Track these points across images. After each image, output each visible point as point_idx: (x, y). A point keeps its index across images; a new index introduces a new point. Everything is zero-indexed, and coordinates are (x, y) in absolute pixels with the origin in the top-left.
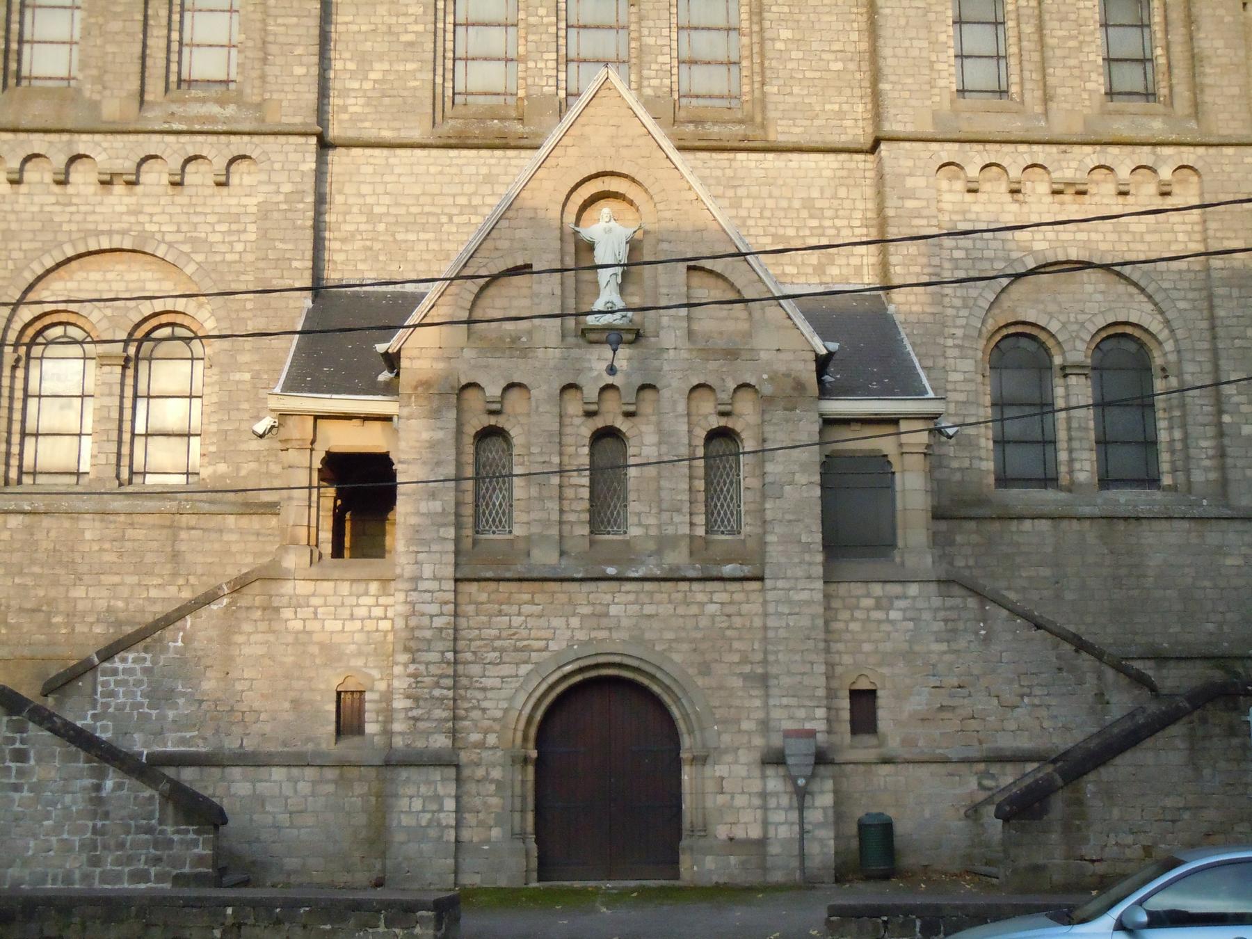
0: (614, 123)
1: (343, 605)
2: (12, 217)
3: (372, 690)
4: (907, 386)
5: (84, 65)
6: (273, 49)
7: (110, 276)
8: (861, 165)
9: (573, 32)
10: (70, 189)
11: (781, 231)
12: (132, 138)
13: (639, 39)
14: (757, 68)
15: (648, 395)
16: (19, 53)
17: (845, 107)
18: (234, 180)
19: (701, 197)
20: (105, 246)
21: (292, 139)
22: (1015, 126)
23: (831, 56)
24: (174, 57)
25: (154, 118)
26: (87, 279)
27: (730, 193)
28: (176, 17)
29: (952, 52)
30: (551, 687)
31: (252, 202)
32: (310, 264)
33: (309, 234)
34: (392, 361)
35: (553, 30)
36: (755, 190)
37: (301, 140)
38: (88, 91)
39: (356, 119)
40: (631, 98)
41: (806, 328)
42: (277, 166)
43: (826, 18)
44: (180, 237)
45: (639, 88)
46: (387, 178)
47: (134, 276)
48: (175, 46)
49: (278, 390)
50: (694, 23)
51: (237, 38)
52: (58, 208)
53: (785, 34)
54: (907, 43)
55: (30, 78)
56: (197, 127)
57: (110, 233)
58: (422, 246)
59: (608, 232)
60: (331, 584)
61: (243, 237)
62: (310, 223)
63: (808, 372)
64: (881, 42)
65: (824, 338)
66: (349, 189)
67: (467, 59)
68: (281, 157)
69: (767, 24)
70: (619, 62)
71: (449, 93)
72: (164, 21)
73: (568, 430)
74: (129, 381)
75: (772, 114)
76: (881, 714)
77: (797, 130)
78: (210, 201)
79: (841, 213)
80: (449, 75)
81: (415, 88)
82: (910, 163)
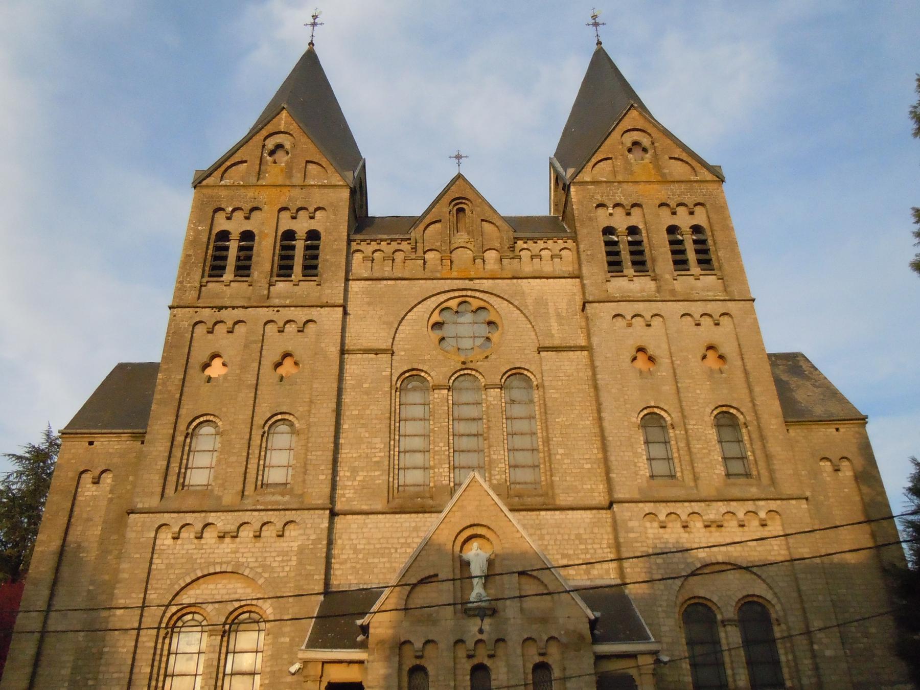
0: (478, 498)
2: (172, 557)
4: (638, 634)
5: (216, 478)
6: (310, 467)
7: (219, 586)
8: (604, 516)
9: (457, 454)
10: (203, 541)
11: (566, 552)
12: (236, 514)
13: (489, 456)
14: (548, 468)
15: (501, 644)
16: (185, 473)
17: (594, 486)
18: (287, 533)
19: (522, 534)
20: (218, 570)
21: (317, 512)
22: (680, 493)
23: (585, 461)
24: (261, 473)
25: (248, 503)
26: (207, 589)
27: (538, 532)
28: (263, 453)
29: (645, 457)
31: (295, 545)
32: (323, 577)
33: (323, 561)
34: (365, 629)
35: (447, 453)
36: (551, 530)
37: (321, 512)
38: (217, 491)
39: (349, 500)
40: (486, 486)
41: (582, 604)
42: (309, 526)
43: (581, 443)
44: (257, 564)
45: (490, 480)
46: (364, 530)
47: (231, 586)
48: (261, 468)
49: (303, 647)
50: (516, 447)
51: (292, 462)
52: (195, 551)
53: (561, 451)
54: (622, 454)
55: (189, 486)
56: (270, 507)
57: (221, 563)
58: (381, 565)
59: (476, 554)
61: (289, 563)
62: (324, 555)
63: (585, 629)
64: (609, 454)
65: (592, 611)
66: (344, 537)
67: (405, 469)
68: (311, 521)
69: (551, 447)
70: (480, 468)
71: (396, 486)
72: (257, 456)
73: (458, 666)
74: (225, 644)
75: (557, 491)
77: (571, 499)
78: (273, 545)
79: (596, 541)
80: (396, 477)
81: (379, 484)
82: (629, 514)
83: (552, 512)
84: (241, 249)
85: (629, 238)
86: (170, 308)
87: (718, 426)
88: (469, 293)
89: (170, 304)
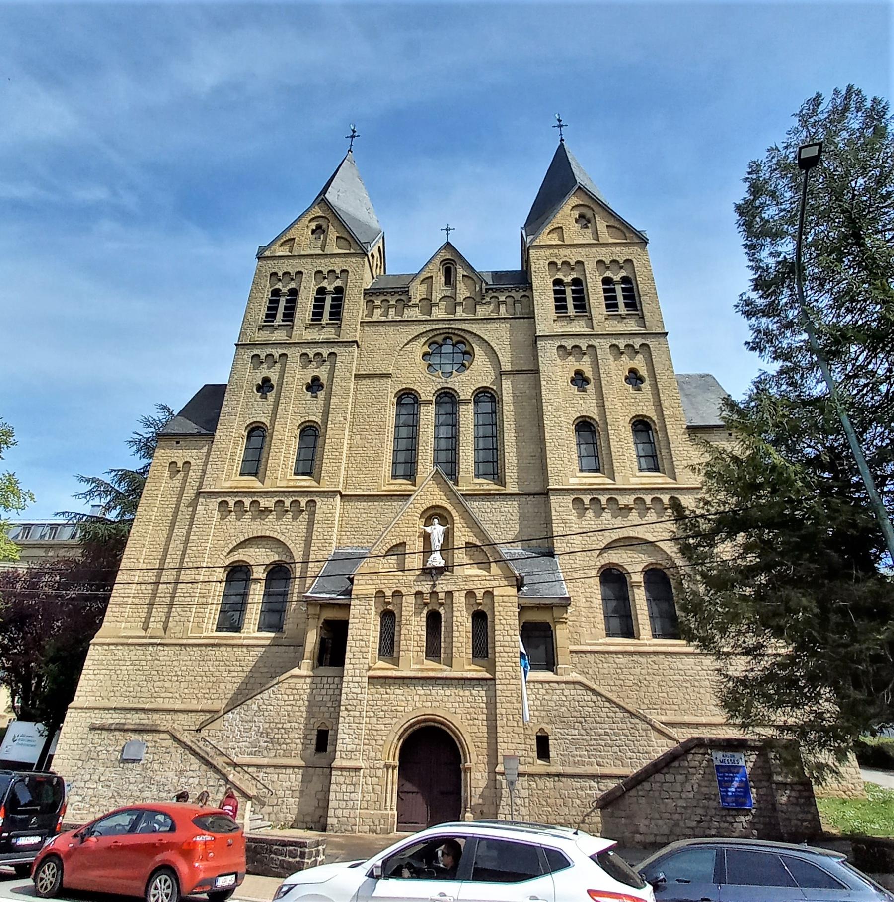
30: (405, 730)
84: (287, 301)
88: (450, 331)
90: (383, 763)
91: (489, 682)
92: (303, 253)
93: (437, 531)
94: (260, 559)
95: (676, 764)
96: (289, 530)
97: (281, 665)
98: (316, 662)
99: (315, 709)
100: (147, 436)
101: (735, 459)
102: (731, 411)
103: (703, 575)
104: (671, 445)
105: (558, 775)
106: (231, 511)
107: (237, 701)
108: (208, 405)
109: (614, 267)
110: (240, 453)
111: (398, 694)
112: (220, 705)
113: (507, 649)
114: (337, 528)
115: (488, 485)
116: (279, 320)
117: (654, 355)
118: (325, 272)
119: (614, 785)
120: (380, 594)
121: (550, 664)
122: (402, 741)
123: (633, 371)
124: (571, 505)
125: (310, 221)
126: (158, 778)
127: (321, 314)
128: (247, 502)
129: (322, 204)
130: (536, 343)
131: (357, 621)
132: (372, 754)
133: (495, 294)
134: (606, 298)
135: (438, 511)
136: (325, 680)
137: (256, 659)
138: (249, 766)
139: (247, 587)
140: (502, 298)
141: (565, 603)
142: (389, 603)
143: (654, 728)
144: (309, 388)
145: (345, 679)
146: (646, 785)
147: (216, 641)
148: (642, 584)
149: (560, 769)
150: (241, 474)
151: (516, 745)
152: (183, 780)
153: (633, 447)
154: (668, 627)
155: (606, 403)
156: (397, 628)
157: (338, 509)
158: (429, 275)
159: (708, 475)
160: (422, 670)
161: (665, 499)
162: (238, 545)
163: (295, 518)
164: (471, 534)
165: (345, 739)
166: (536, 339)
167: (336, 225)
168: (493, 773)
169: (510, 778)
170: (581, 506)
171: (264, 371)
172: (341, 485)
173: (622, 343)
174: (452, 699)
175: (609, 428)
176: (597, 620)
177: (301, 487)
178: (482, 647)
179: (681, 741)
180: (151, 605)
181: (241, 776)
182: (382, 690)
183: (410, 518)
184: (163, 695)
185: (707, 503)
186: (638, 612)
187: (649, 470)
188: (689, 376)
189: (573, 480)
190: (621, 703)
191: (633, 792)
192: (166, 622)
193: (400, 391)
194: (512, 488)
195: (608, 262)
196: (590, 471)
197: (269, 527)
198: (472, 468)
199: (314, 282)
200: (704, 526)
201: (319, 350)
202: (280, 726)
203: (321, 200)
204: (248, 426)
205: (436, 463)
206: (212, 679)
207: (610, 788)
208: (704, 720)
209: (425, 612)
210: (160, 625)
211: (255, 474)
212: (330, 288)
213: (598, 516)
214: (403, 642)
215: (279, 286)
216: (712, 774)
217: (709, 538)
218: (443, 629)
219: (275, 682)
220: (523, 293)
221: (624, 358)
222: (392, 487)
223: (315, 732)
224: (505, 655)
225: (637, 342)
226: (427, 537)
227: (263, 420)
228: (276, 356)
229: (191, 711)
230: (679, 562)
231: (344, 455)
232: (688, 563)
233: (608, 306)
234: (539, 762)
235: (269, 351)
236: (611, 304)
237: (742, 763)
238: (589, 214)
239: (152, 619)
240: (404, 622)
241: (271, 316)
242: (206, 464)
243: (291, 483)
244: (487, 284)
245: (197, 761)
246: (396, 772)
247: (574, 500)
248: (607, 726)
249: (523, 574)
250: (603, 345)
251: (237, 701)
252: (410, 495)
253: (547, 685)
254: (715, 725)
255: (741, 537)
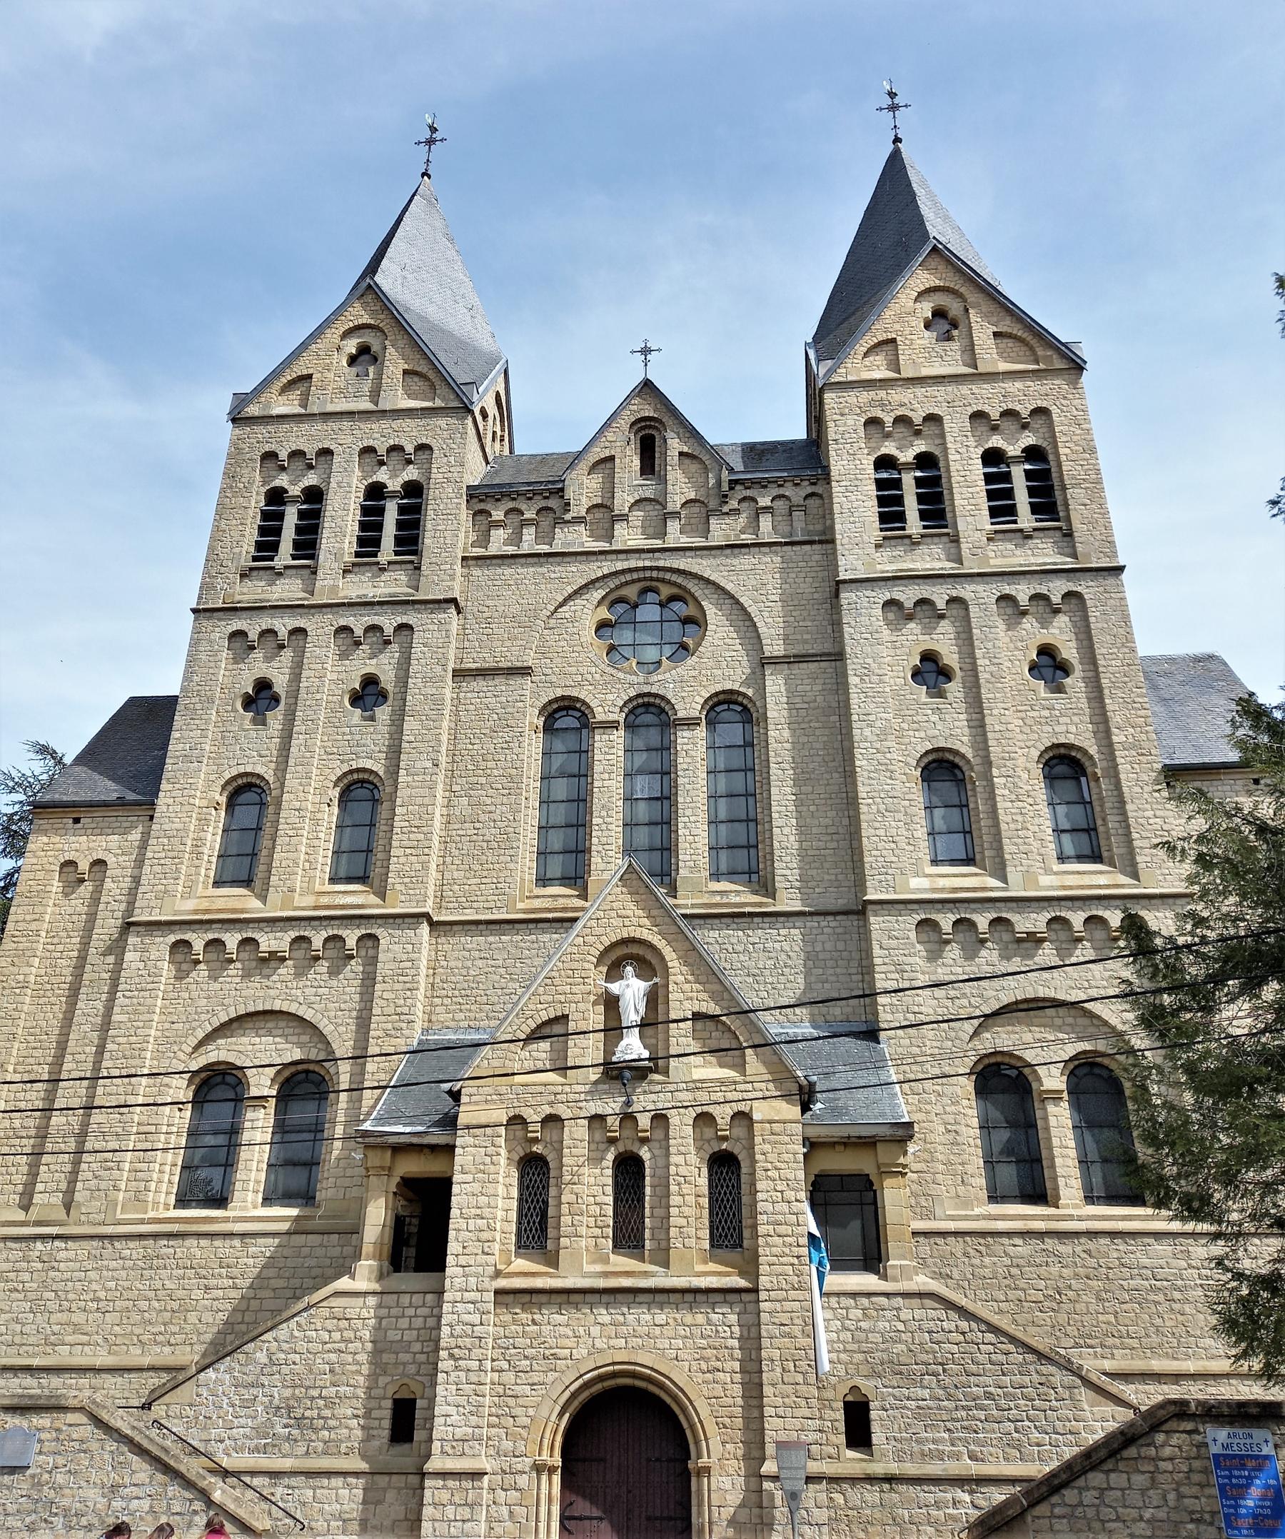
1: (403, 1316)
3: (422, 1398)
8: (855, 923)
30: (574, 1395)
60: (395, 1296)
76: (875, 1427)
83: (773, 919)
85: (919, 474)
86: (194, 611)
87: (1051, 778)
88: (655, 574)
89: (194, 606)
90: (529, 1461)
91: (745, 1297)
92: (330, 408)
93: (632, 990)
94: (262, 1058)
95: (1132, 1452)
96: (324, 999)
97: (315, 1272)
98: (386, 1264)
99: (386, 1357)
100: (9, 810)
101: (1262, 829)
102: (1255, 727)
103: (1190, 1069)
104: (1129, 807)
105: (890, 1479)
106: (197, 962)
107: (218, 1353)
108: (138, 739)
109: (1007, 425)
110: (213, 840)
111: (556, 1322)
112: (189, 1356)
113: (782, 1229)
114: (421, 990)
115: (740, 896)
116: (285, 555)
117: (1094, 614)
118: (382, 450)
119: (1004, 1497)
120: (517, 1121)
121: (872, 1257)
122: (567, 1415)
123: (1046, 651)
124: (913, 935)
125: (346, 335)
126: (65, 1502)
127: (377, 542)
128: (232, 940)
129: (369, 298)
130: (837, 596)
131: (469, 1178)
132: (507, 1445)
133: (748, 493)
134: (991, 495)
135: (635, 950)
136: (405, 1299)
137: (261, 1261)
138: (253, 1473)
139: (237, 1114)
140: (764, 501)
141: (903, 1133)
142: (536, 1140)
143: (1087, 1383)
144: (357, 699)
145: (447, 1296)
146: (1070, 1495)
147: (175, 1228)
148: (1065, 1095)
149: (894, 1468)
150: (217, 884)
151: (801, 1422)
152: (117, 1504)
153: (1045, 810)
154: (1122, 1181)
155: (988, 720)
156: (553, 1191)
157: (425, 952)
158: (607, 453)
159: (1203, 861)
160: (606, 1275)
161: (1115, 918)
162: (215, 1030)
163: (334, 972)
164: (705, 996)
165: (450, 1415)
166: (838, 586)
167: (401, 344)
168: (755, 1476)
169: (788, 1485)
170: (934, 936)
171: (258, 666)
172: (430, 902)
173: (1022, 592)
174: (668, 1331)
175: (995, 772)
176: (970, 1169)
177: (343, 907)
178: (730, 1226)
179: (1143, 1408)
180: (37, 1154)
181: (237, 1493)
182: (525, 1317)
183: (576, 965)
184: (69, 1339)
185: (1200, 922)
186: (1056, 1152)
187: (1080, 858)
188: (1171, 660)
189: (915, 882)
190: (1020, 1335)
191: (1042, 1509)
192: (70, 1192)
193: (550, 702)
194: (788, 901)
195: (995, 414)
196: (953, 862)
197: (281, 990)
198: (704, 861)
199: (358, 473)
200: (1194, 970)
201: (376, 620)
202: (315, 1393)
203: (367, 288)
204: (228, 783)
205: (628, 850)
206: (175, 1305)
207: (995, 1503)
208: (1190, 1366)
209: (610, 1156)
210: (57, 1199)
211: (247, 883)
212: (394, 485)
213: (970, 955)
214: (566, 1220)
215: (282, 481)
216: (1205, 1471)
217: (1202, 997)
218: (648, 1190)
219: (301, 1306)
220: (810, 490)
221: (1028, 624)
222: (537, 903)
223: (388, 1404)
224: (779, 1241)
225: (1056, 589)
226: (611, 1003)
227: (259, 770)
228: (283, 633)
229: (130, 1370)
230: (1140, 1041)
231: (436, 839)
232: (1159, 1044)
233: (994, 512)
234: (850, 1454)
235: (266, 622)
236: (1001, 507)
237: (1267, 1450)
238: (954, 308)
239: (40, 1187)
240: (567, 1178)
241: (267, 546)
242: (140, 863)
243: (325, 900)
244: (731, 470)
245: (146, 1466)
246: (557, 1479)
247: (920, 923)
248: (989, 1381)
249: (815, 1078)
250: (981, 596)
251: (218, 1353)
252: (575, 920)
253: (865, 1301)
254: (1215, 1376)
255: (1270, 991)
